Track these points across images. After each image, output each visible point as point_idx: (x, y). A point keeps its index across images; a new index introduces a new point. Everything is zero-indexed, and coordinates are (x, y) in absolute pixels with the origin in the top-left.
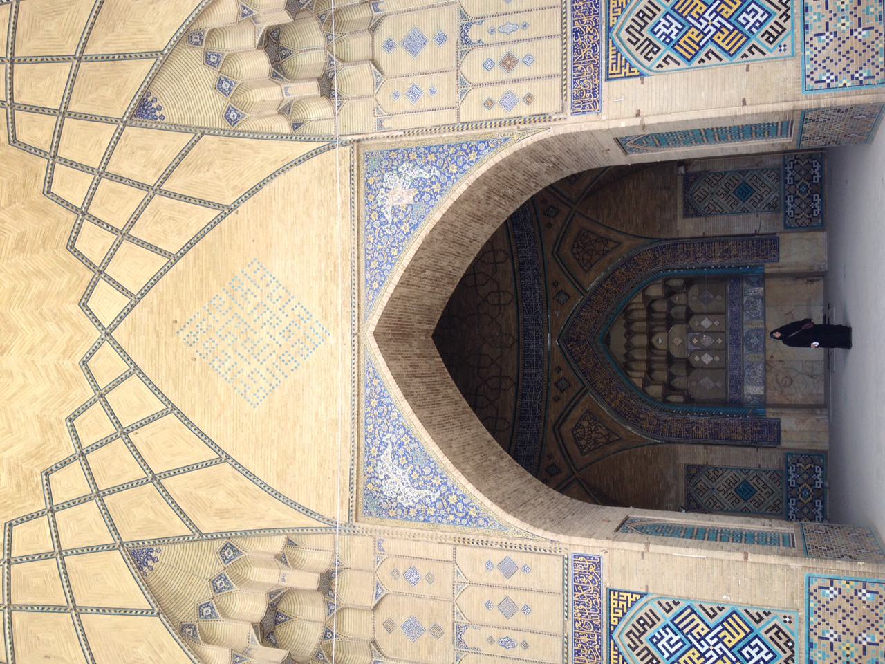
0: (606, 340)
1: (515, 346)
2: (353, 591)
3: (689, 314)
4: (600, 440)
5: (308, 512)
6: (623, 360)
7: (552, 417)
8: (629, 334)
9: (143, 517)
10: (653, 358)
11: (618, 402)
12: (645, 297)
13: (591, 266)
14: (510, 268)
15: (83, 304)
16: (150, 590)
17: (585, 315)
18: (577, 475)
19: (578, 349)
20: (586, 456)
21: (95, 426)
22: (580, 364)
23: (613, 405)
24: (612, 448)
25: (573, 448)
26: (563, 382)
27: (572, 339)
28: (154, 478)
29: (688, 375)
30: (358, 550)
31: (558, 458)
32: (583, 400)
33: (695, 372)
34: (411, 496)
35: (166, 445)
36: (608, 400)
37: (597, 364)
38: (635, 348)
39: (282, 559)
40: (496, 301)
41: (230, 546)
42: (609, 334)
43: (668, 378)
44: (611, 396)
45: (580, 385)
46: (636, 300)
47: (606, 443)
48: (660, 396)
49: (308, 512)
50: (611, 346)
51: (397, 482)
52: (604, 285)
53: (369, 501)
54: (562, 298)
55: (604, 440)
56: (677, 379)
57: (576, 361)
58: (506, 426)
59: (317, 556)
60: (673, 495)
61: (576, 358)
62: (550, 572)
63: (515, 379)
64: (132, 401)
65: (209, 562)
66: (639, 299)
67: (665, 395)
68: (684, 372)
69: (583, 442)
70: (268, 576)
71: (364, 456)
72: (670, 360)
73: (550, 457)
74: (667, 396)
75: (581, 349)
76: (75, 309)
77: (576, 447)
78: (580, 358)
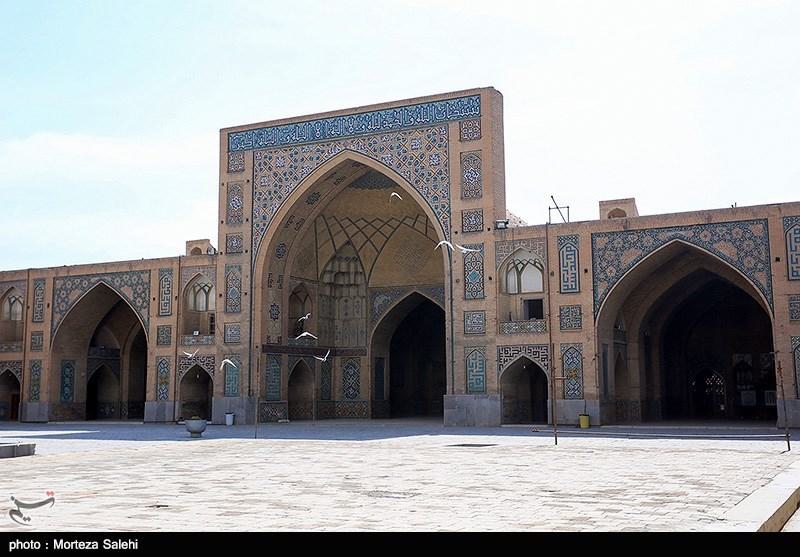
2: (353, 291)
5: (370, 276)
9: (359, 240)
15: (406, 217)
16: (341, 248)
21: (378, 224)
26: (598, 239)
28: (369, 240)
30: (362, 292)
34: (376, 305)
35: (378, 240)
39: (356, 273)
41: (357, 259)
49: (370, 276)
51: (380, 300)
53: (374, 293)
59: (360, 280)
62: (362, 344)
64: (387, 230)
65: (351, 255)
70: (352, 270)
71: (384, 291)
76: (405, 215)
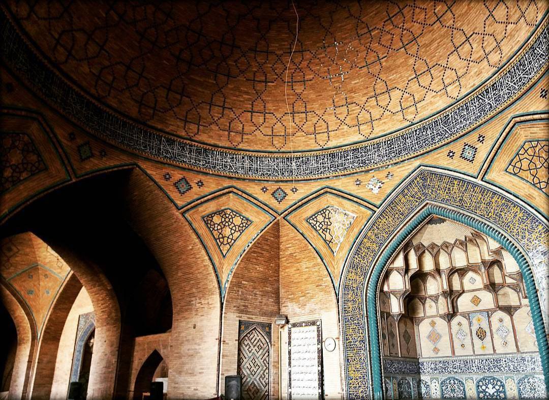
0: (431, 219)
1: (408, 123)
3: (509, 310)
4: (327, 234)
6: (426, 244)
7: (339, 184)
8: (463, 244)
10: (444, 276)
11: (368, 245)
12: (497, 252)
13: (515, 174)
14: (486, 76)
17: (455, 187)
18: (279, 218)
19: (416, 189)
20: (304, 223)
22: (401, 196)
23: (365, 240)
24: (320, 245)
25: (310, 210)
27: (425, 180)
29: (441, 317)
31: (292, 198)
32: (363, 209)
33: (445, 323)
36: (369, 234)
37: (402, 214)
38: (450, 255)
40: (447, 82)
42: (443, 221)
43: (431, 297)
44: (373, 237)
45: (378, 203)
46: (491, 241)
47: (325, 241)
48: (392, 288)
50: (430, 226)
52: (495, 199)
54: (469, 154)
55: (328, 238)
56: (433, 304)
57: (403, 191)
58: (321, 143)
60: (298, 310)
61: (406, 191)
63: (372, 136)
66: (494, 245)
67: (394, 293)
68: (442, 312)
69: (320, 218)
72: (452, 295)
73: (294, 190)
74: (393, 294)
75: (416, 193)
77: (313, 212)
78: (407, 195)
